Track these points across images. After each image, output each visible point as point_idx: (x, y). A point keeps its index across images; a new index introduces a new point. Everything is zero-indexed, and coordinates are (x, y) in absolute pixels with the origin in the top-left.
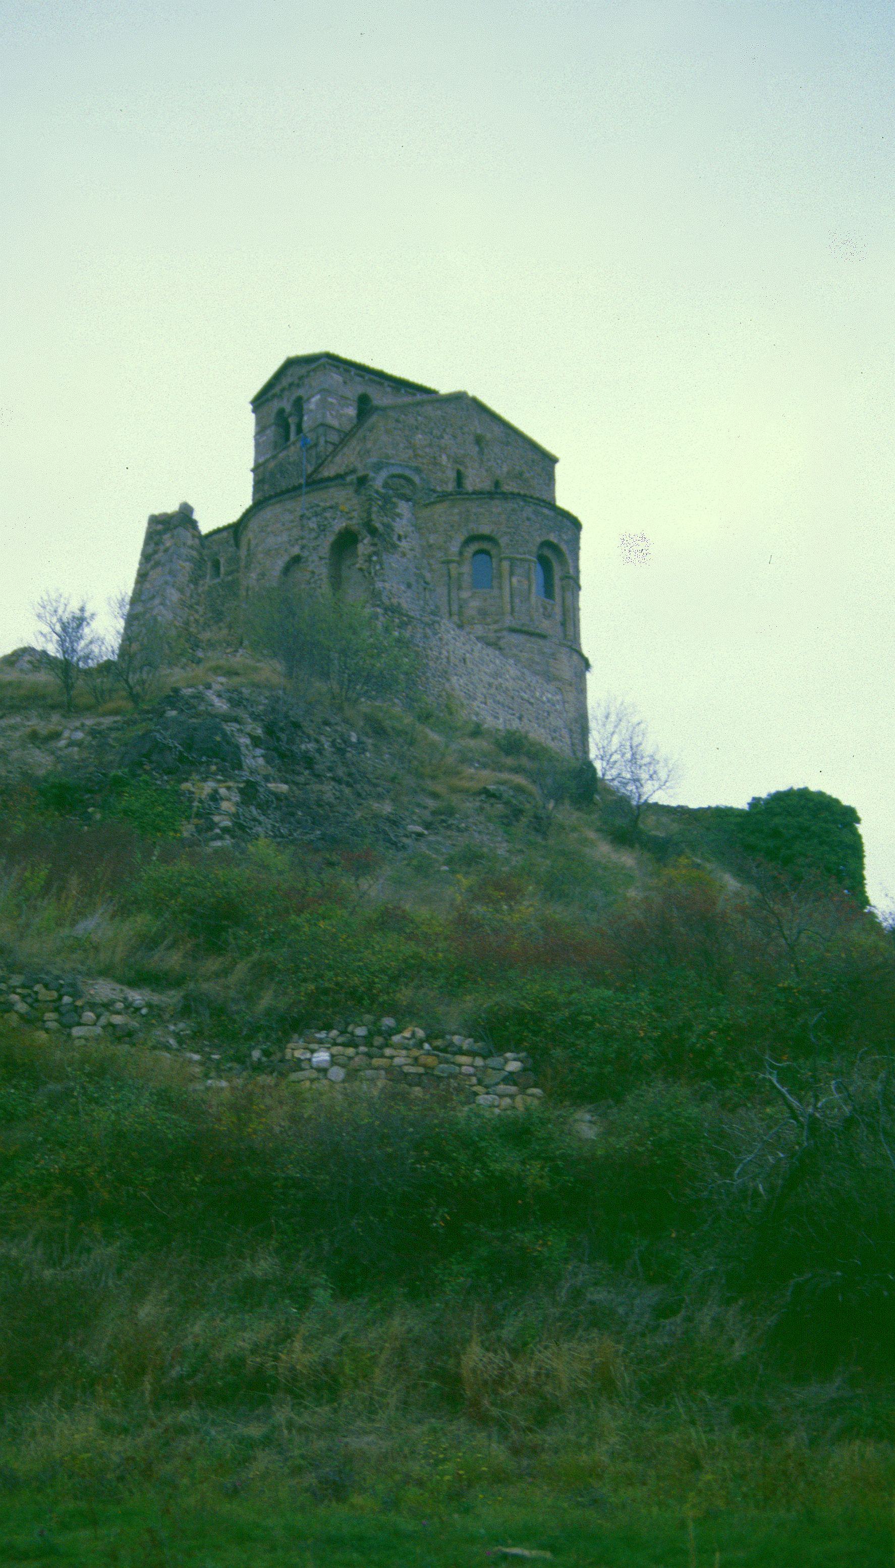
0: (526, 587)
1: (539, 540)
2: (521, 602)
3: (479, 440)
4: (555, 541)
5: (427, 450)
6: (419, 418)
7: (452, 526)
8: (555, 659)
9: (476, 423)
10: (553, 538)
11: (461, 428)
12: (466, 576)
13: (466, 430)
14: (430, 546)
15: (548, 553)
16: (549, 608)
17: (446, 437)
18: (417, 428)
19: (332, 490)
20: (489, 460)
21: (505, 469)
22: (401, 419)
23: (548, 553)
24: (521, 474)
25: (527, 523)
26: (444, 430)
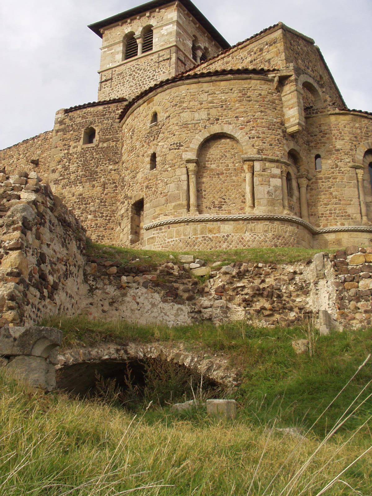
7: (356, 137)
14: (338, 150)
19: (253, 81)
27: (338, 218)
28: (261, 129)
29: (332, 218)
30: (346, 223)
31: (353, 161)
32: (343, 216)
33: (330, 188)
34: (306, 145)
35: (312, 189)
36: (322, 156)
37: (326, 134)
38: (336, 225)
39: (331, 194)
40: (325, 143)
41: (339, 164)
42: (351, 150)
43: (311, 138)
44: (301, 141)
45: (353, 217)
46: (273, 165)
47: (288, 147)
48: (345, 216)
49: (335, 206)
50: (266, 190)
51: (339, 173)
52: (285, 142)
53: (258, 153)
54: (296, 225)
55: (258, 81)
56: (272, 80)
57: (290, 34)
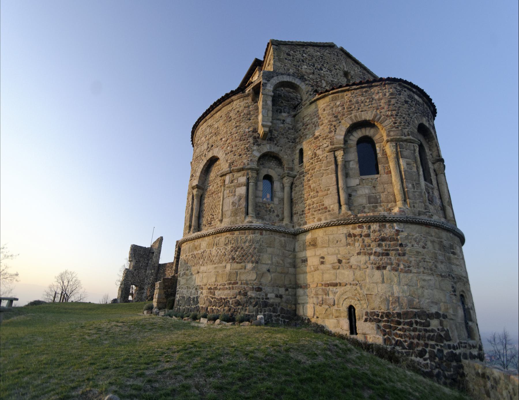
5: (311, 76)
6: (304, 55)
9: (344, 64)
11: (334, 67)
13: (337, 67)
17: (324, 69)
26: (323, 65)
27: (315, 213)
28: (234, 144)
29: (310, 214)
30: (323, 218)
31: (332, 143)
32: (319, 210)
33: (309, 180)
34: (293, 142)
35: (296, 186)
36: (304, 150)
37: (307, 125)
38: (313, 221)
39: (310, 187)
40: (307, 135)
41: (319, 152)
42: (330, 132)
43: (297, 135)
44: (283, 141)
45: (330, 209)
46: (240, 174)
47: (260, 152)
48: (322, 209)
49: (313, 200)
50: (231, 201)
51: (317, 162)
52: (255, 148)
53: (230, 166)
54: (259, 231)
55: (238, 100)
56: (248, 95)
57: (287, 46)
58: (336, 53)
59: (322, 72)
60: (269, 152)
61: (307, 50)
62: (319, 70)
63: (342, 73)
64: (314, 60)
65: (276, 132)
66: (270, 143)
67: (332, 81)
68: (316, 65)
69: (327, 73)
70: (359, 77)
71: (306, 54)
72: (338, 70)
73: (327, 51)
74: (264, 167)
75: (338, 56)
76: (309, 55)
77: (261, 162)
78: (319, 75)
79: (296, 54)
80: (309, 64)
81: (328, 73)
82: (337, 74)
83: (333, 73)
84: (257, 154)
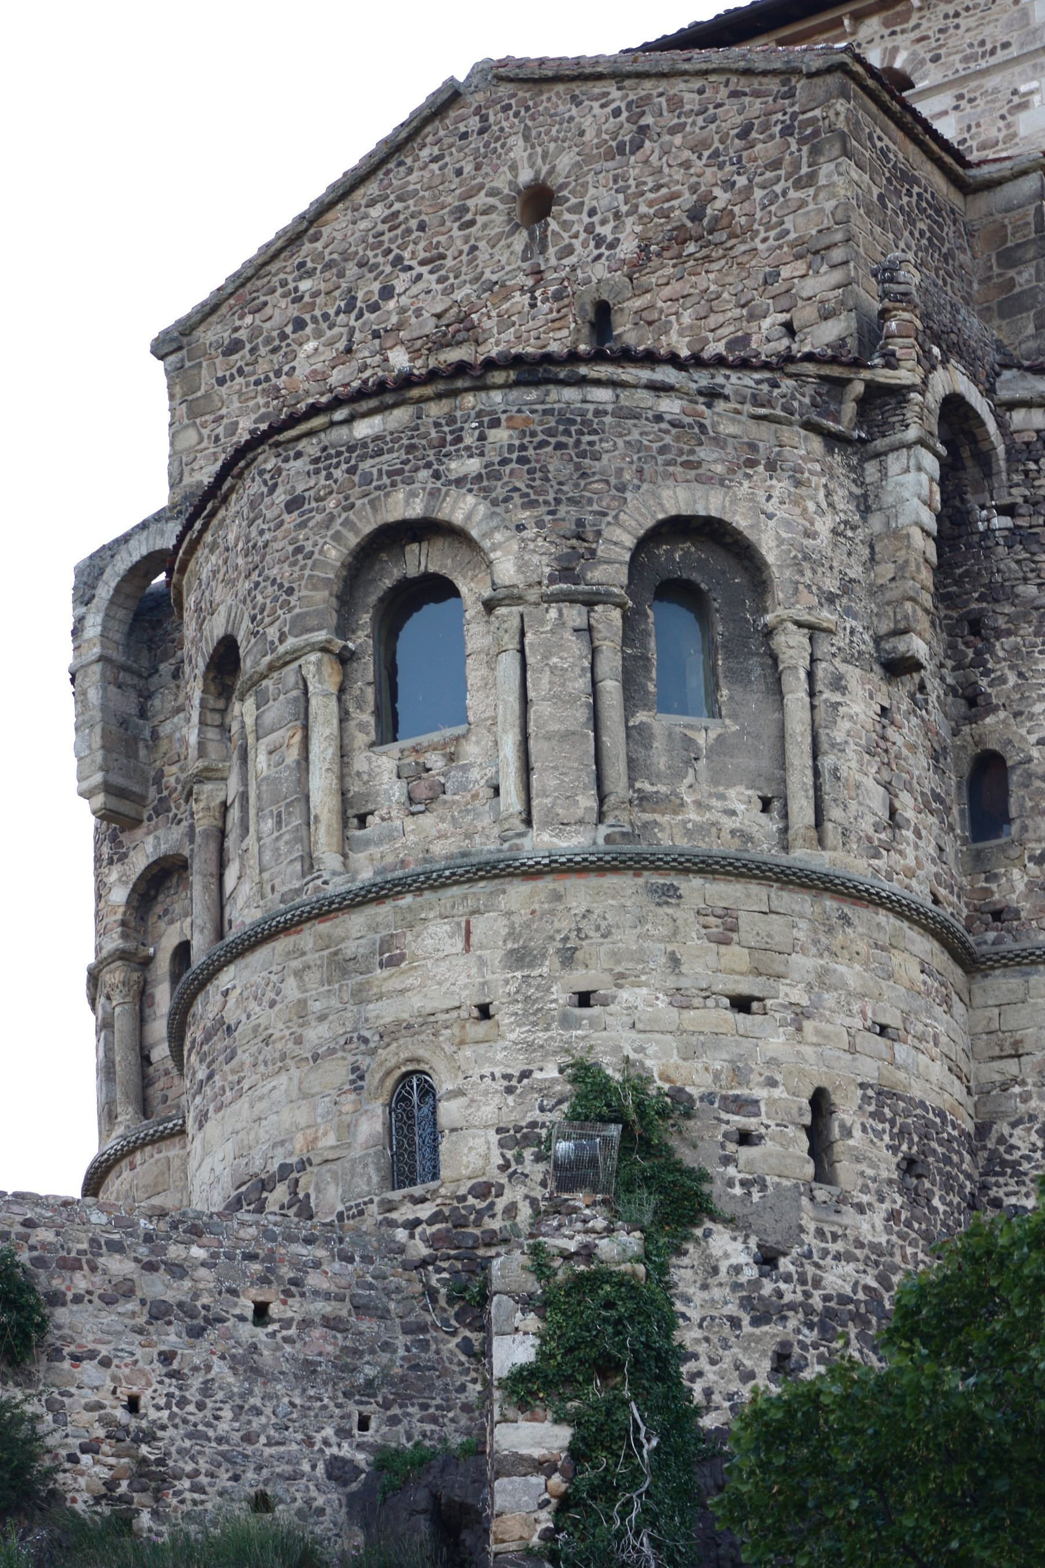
0: (293, 755)
1: (335, 554)
2: (279, 823)
3: (538, 202)
4: (416, 510)
6: (305, 285)
8: (393, 962)
9: (518, 150)
10: (404, 506)
12: (236, 805)
15: (420, 560)
16: (435, 761)
17: (401, 282)
18: (299, 324)
20: (569, 250)
21: (628, 248)
22: (243, 334)
23: (420, 560)
24: (696, 214)
25: (291, 519)
26: (399, 259)
58: (474, 123)
59: (392, 304)
60: (155, 862)
61: (319, 245)
62: (374, 308)
63: (498, 219)
64: (352, 270)
65: (174, 769)
66: (156, 828)
67: (439, 316)
68: (360, 295)
69: (415, 290)
70: (609, 156)
71: (310, 274)
72: (481, 220)
73: (425, 154)
74: (171, 922)
75: (481, 132)
76: (328, 266)
77: (158, 909)
78: (376, 335)
79: (268, 311)
80: (326, 317)
81: (430, 280)
82: (474, 248)
83: (449, 262)
84: (119, 895)
